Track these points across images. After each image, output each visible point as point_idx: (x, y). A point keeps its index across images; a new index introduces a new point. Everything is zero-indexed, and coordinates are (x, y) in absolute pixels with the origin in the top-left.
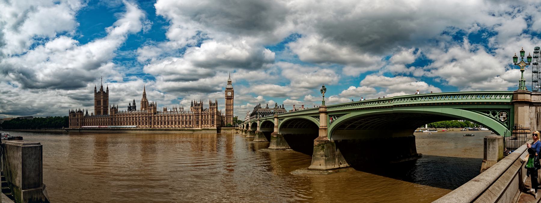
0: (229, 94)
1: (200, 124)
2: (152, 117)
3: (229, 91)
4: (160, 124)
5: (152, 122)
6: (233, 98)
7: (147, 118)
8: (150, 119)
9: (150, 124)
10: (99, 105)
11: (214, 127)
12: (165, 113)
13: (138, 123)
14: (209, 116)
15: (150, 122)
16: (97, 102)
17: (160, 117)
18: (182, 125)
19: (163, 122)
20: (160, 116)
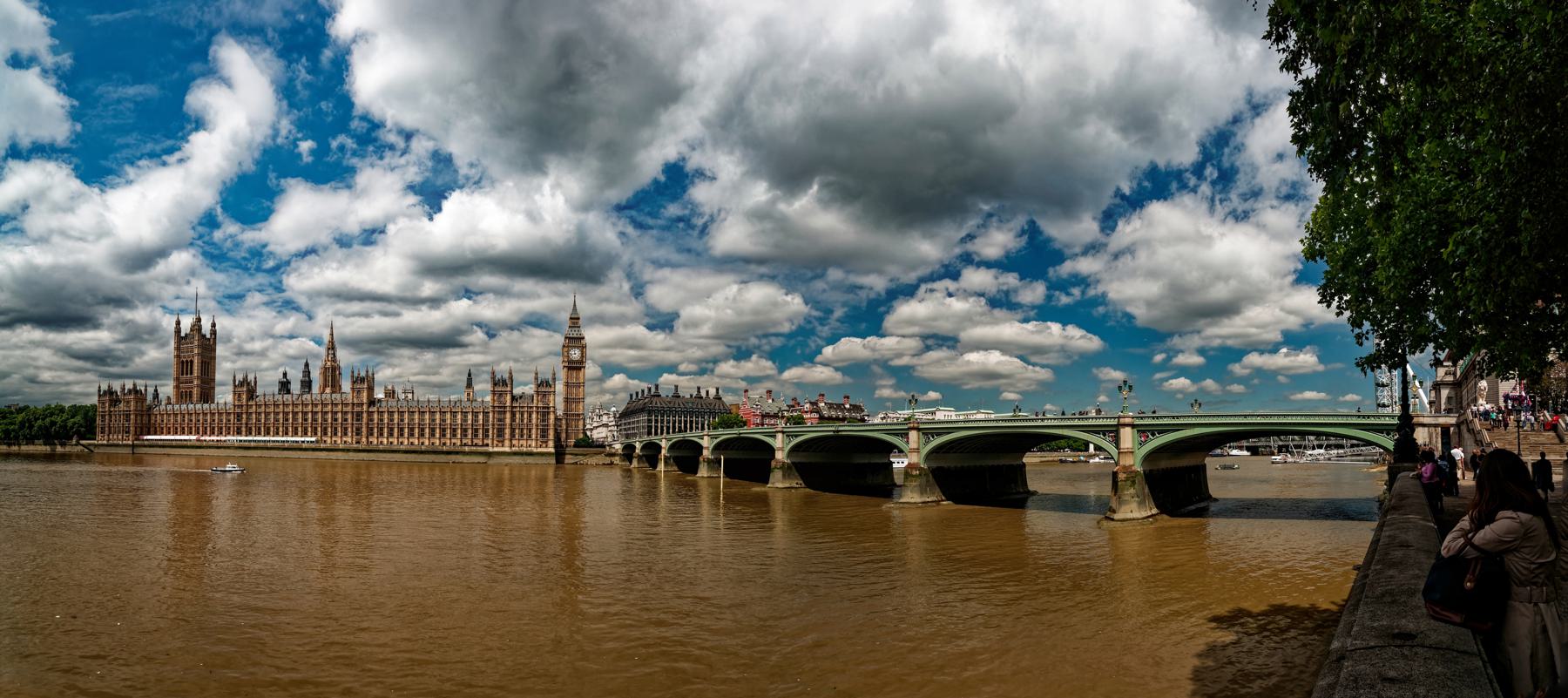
0: (575, 354)
1: (507, 436)
2: (362, 412)
3: (575, 347)
4: (385, 435)
5: (364, 429)
6: (584, 367)
7: (349, 416)
8: (358, 420)
9: (357, 434)
10: (187, 374)
11: (547, 446)
12: (392, 403)
13: (319, 429)
14: (534, 416)
15: (358, 429)
16: (183, 366)
17: (386, 415)
18: (450, 439)
19: (396, 430)
20: (388, 412)
